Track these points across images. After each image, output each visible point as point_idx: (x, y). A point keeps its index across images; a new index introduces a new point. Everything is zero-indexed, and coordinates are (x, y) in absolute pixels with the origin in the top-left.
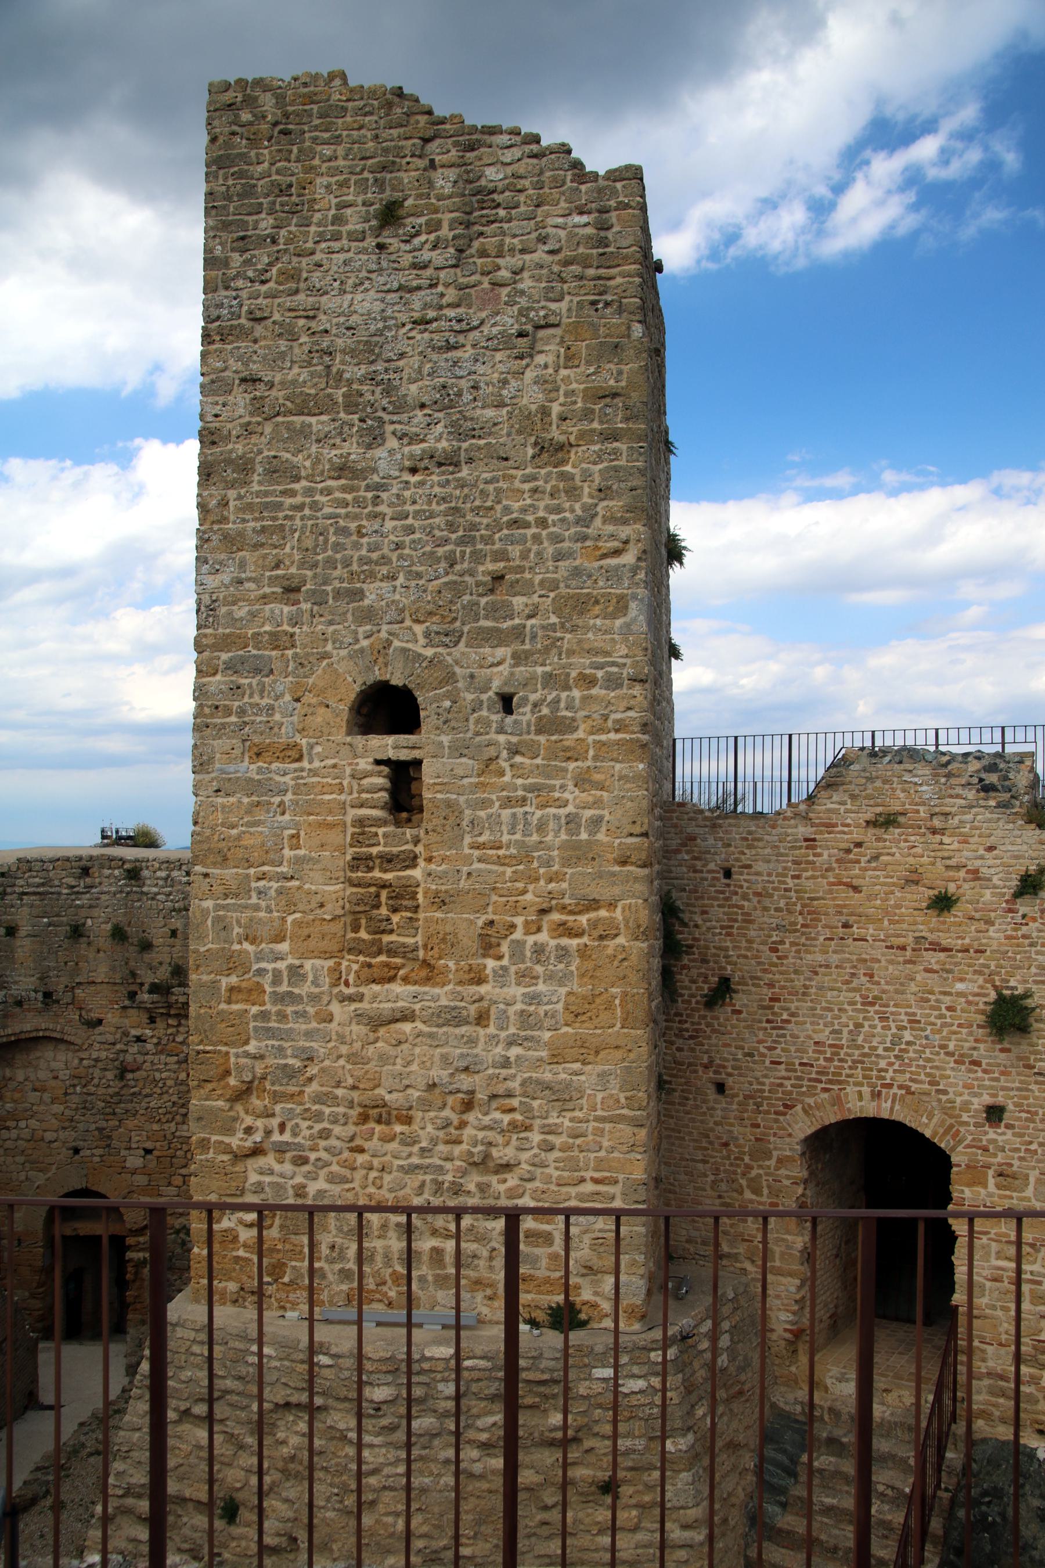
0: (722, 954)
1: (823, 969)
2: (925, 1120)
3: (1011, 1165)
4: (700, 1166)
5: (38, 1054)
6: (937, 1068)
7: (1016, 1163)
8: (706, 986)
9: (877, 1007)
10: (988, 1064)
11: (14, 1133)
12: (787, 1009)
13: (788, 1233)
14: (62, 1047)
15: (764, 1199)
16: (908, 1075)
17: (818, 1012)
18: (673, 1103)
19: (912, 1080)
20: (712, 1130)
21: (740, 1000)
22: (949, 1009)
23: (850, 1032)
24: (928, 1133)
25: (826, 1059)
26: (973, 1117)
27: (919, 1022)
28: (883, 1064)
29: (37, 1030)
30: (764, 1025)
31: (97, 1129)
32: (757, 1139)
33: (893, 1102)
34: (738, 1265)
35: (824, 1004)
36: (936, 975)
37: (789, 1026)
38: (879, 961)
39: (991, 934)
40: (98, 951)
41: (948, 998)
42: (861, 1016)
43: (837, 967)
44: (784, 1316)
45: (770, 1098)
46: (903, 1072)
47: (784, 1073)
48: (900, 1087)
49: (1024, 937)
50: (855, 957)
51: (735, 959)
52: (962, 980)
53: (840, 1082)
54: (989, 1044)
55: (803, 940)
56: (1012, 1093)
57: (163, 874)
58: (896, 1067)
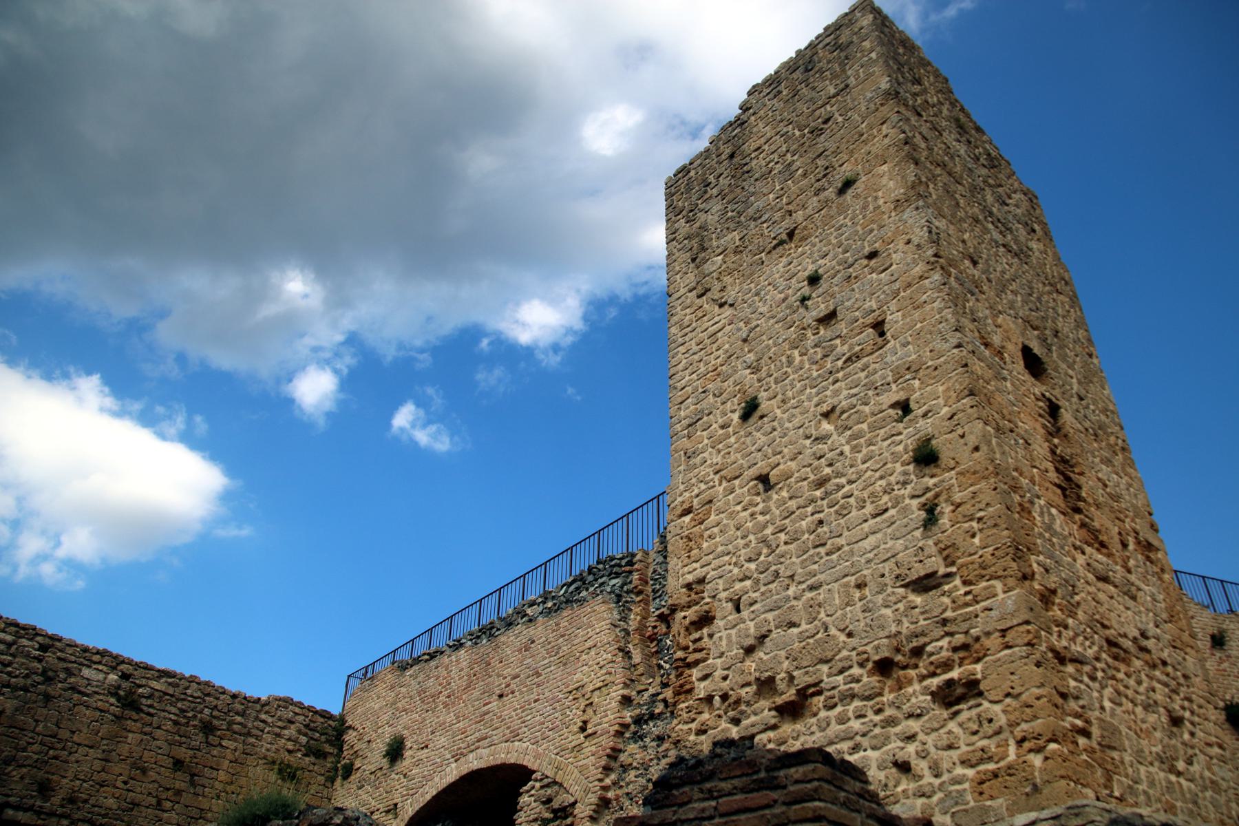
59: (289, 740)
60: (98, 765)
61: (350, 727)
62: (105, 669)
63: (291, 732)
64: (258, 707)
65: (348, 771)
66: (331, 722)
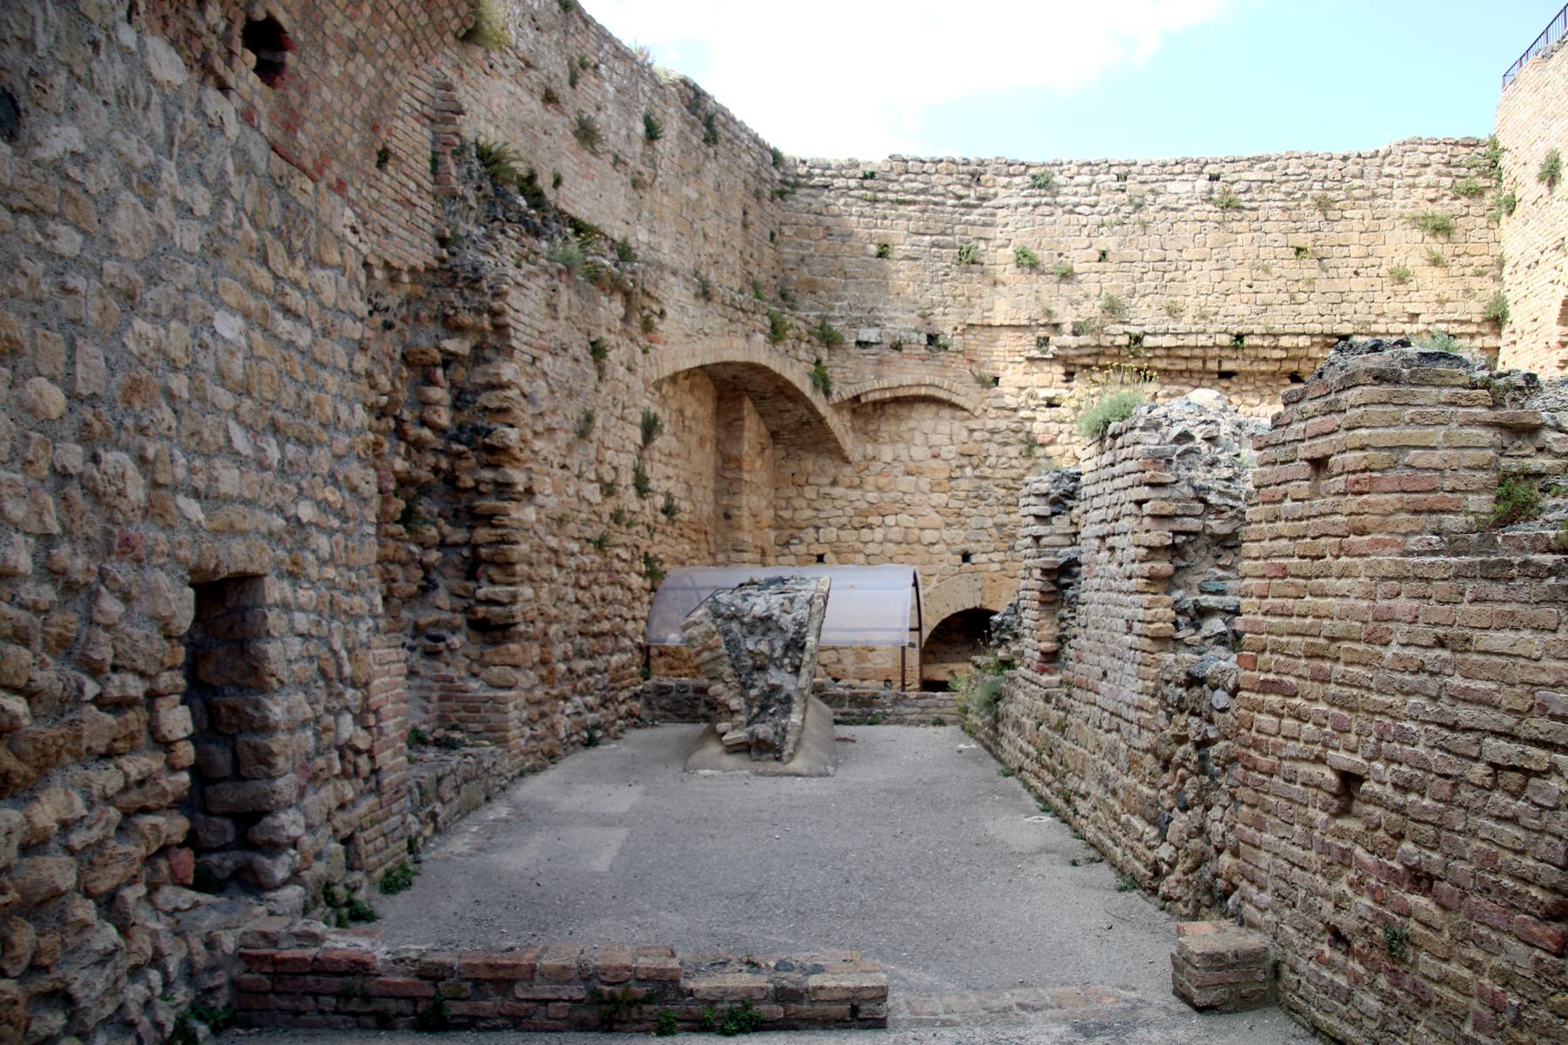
5: (912, 424)
11: (879, 534)
14: (946, 413)
29: (919, 385)
31: (995, 525)
40: (995, 284)
57: (1086, 179)
59: (1428, 187)
60: (1216, 276)
61: (1504, 150)
62: (1190, 177)
63: (1429, 176)
64: (1378, 161)
65: (1511, 206)
66: (1481, 150)
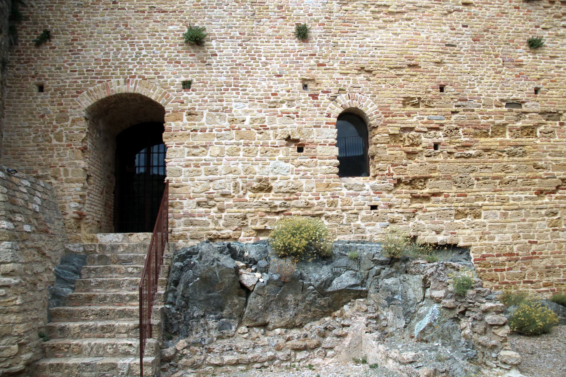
0: (46, 19)
1: (101, 24)
2: (152, 91)
3: (195, 108)
4: (27, 130)
6: (159, 66)
7: (197, 107)
8: (36, 36)
9: (129, 40)
10: (184, 62)
12: (81, 44)
13: (77, 159)
15: (64, 143)
16: (143, 71)
17: (98, 44)
18: (13, 98)
19: (145, 73)
20: (35, 109)
21: (55, 42)
22: (165, 38)
23: (114, 53)
24: (153, 98)
25: (101, 67)
26: (176, 87)
27: (150, 45)
28: (131, 67)
30: (68, 53)
32: (61, 112)
33: (136, 84)
34: (47, 181)
35: (101, 41)
36: (159, 24)
37: (82, 53)
38: (131, 19)
39: (186, 4)
41: (165, 34)
42: (120, 45)
43: (109, 22)
44: (73, 205)
45: (69, 89)
46: (141, 69)
47: (77, 76)
48: (139, 77)
49: (202, 4)
50: (118, 17)
51: (53, 21)
52: (172, 25)
53: (108, 78)
54: (185, 53)
55: (91, 10)
56: (195, 75)
58: (138, 67)
